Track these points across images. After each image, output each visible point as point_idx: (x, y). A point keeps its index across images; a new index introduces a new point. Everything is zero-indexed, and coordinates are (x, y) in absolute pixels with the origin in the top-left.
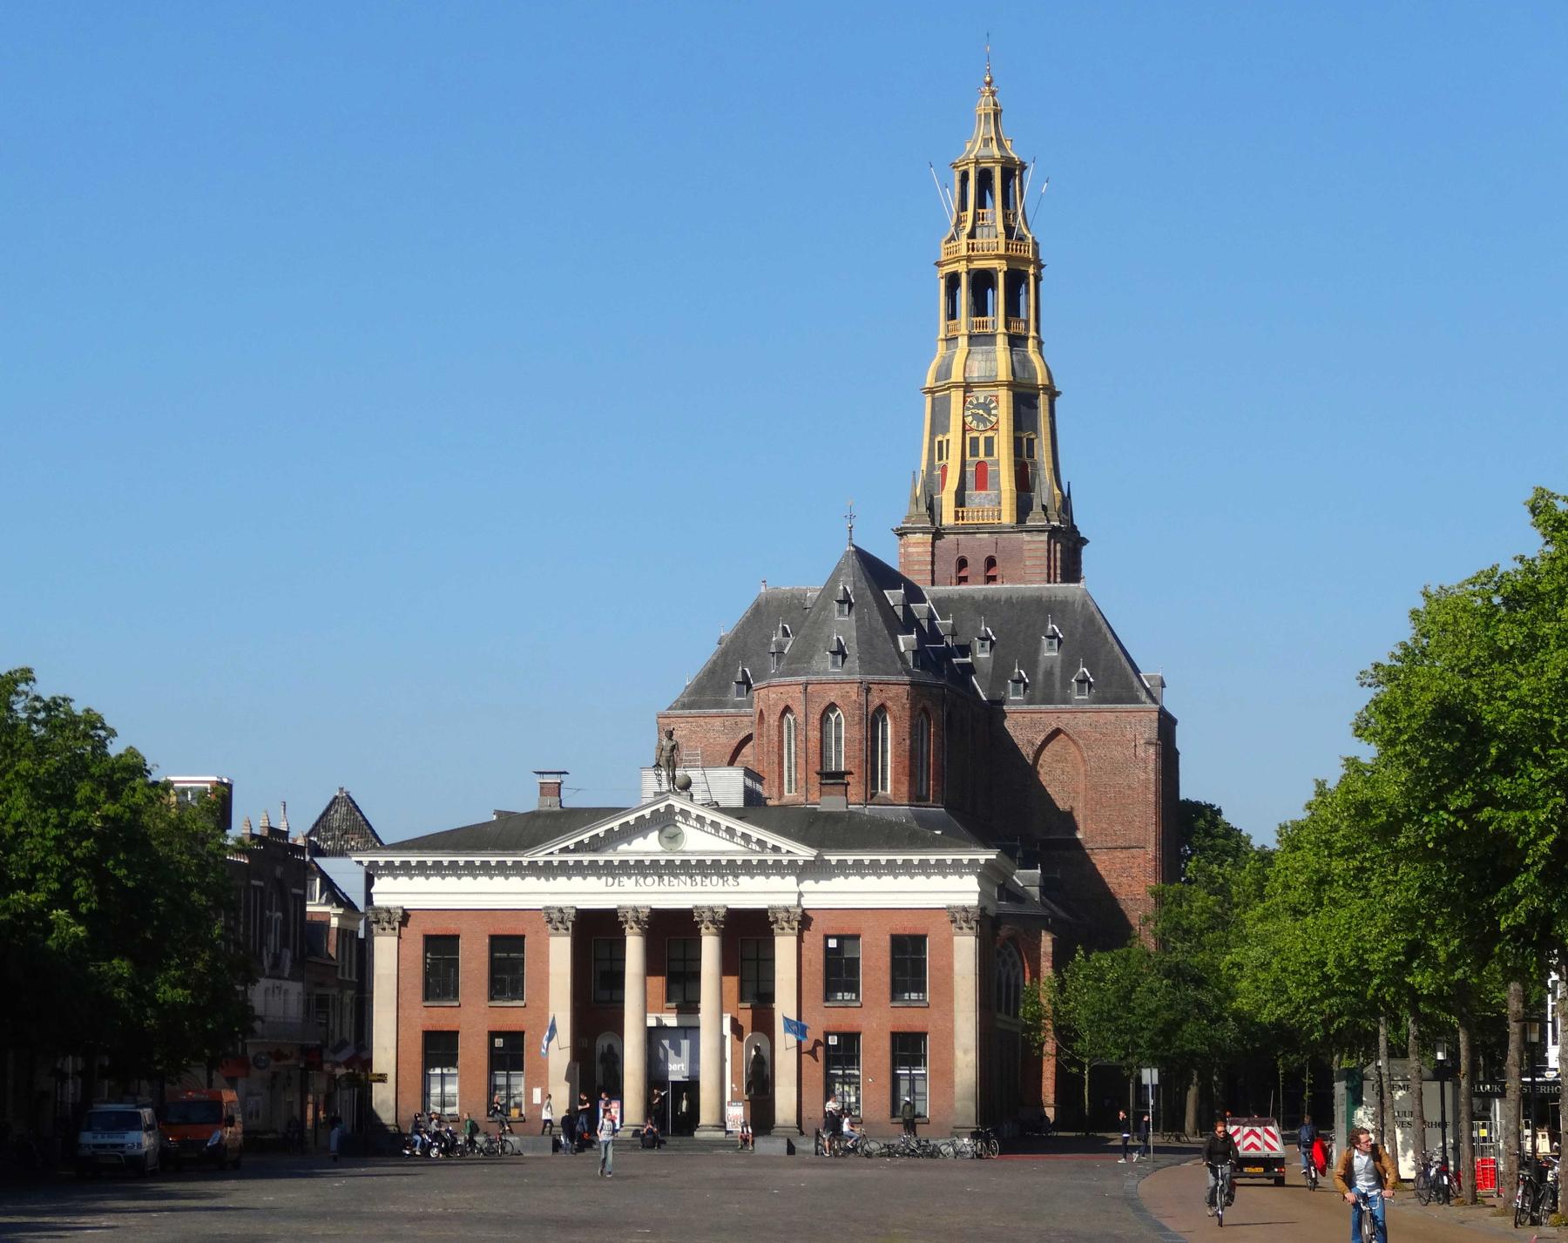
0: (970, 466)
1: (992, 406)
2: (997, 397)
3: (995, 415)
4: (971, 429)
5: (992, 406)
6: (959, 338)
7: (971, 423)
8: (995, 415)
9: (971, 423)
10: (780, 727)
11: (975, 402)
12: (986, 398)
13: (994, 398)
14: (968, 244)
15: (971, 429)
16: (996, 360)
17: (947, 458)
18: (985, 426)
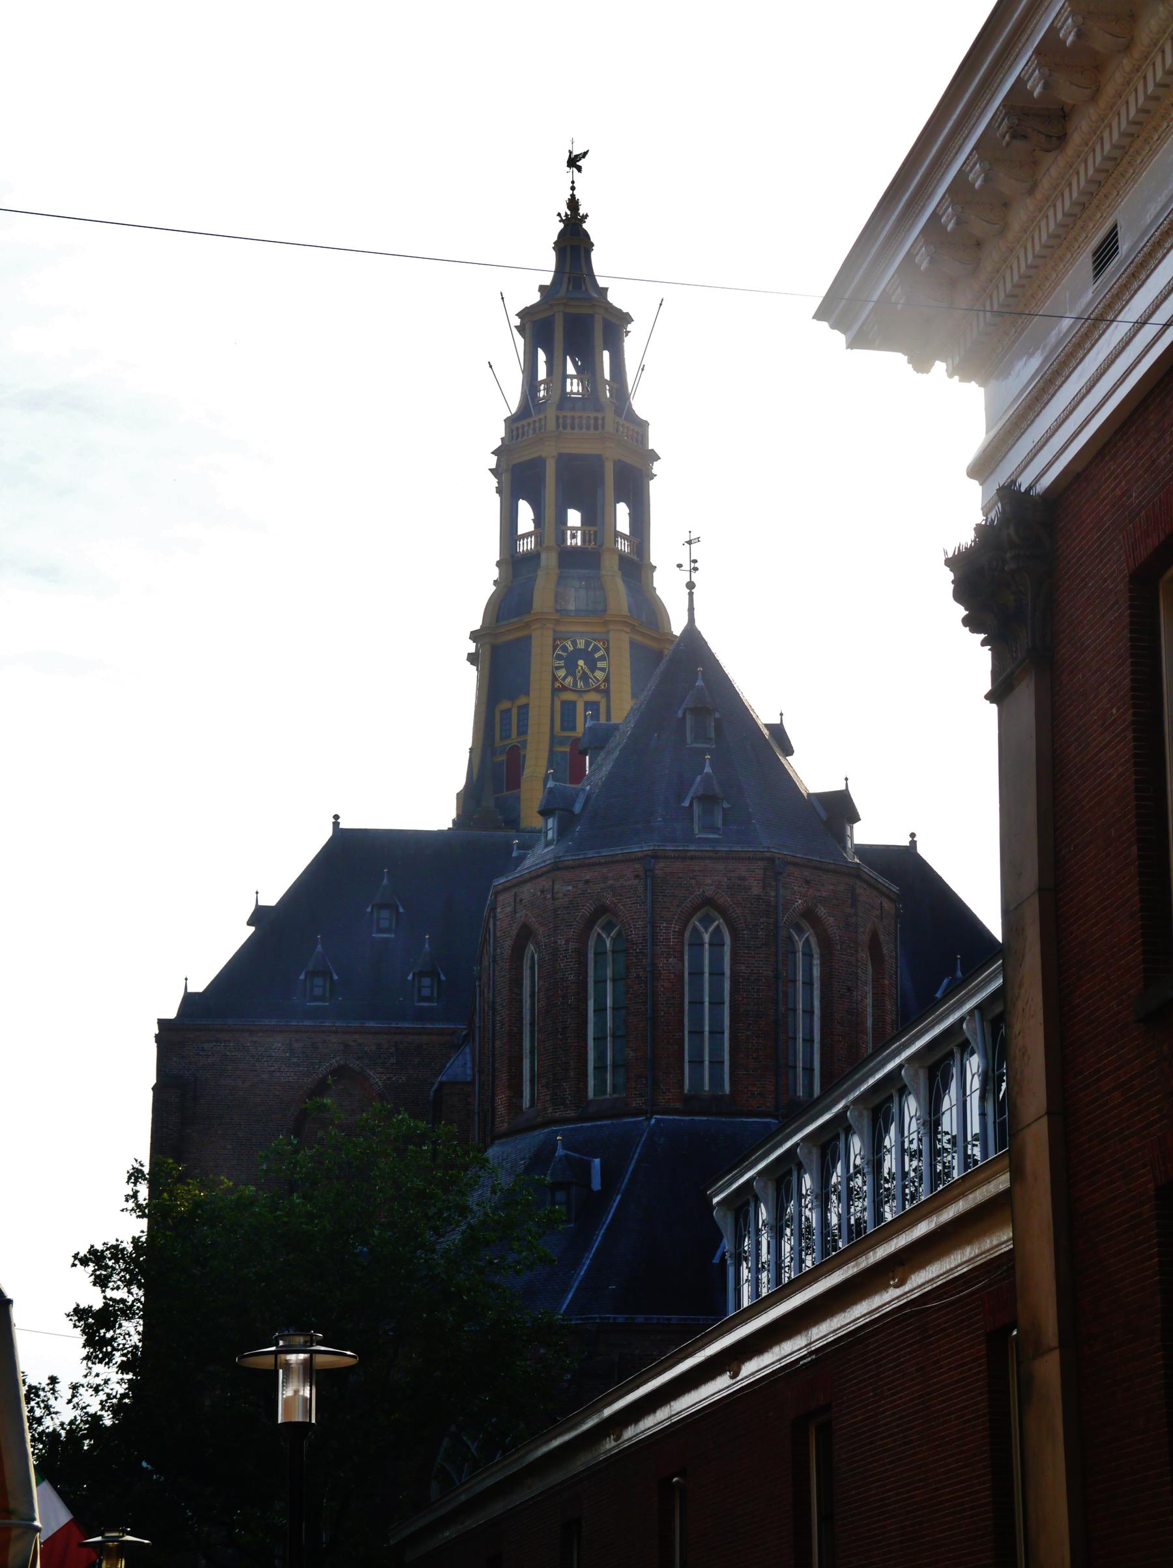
0: (562, 744)
1: (597, 656)
2: (606, 642)
3: (602, 670)
4: (564, 689)
5: (597, 656)
6: (543, 556)
7: (564, 678)
8: (602, 670)
9: (564, 678)
10: (581, 954)
11: (571, 649)
12: (587, 644)
13: (600, 645)
14: (557, 418)
15: (564, 689)
16: (602, 588)
17: (523, 730)
18: (586, 683)
